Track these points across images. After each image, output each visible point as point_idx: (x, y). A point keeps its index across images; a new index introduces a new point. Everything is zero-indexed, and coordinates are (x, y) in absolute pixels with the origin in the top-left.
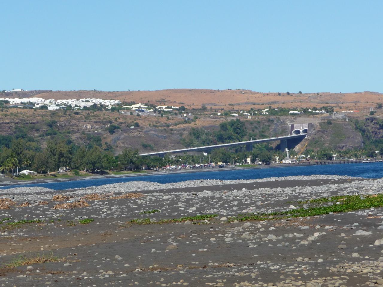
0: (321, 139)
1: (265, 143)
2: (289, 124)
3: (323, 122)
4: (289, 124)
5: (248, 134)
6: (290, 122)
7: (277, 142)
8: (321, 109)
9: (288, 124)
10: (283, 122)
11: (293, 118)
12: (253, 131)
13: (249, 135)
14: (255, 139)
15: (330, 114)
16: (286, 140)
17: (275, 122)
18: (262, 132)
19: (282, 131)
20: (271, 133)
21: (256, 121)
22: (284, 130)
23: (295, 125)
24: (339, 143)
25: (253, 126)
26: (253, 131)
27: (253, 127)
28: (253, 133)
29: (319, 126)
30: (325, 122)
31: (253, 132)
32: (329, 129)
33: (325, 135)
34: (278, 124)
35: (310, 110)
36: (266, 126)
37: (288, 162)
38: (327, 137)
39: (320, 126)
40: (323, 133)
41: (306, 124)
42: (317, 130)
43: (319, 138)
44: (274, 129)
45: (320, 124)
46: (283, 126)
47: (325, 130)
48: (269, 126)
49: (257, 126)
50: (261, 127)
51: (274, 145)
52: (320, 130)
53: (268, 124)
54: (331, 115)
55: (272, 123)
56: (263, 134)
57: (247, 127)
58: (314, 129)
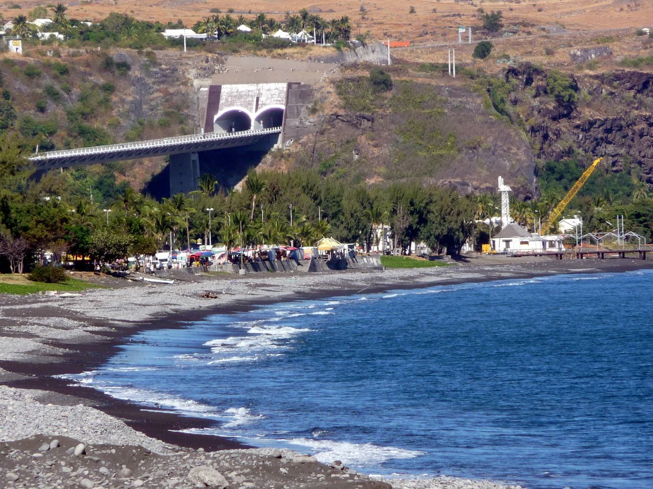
0: (346, 156)
1: (97, 169)
2: (202, 86)
3: (352, 80)
4: (202, 86)
5: (17, 124)
6: (198, 76)
7: (146, 161)
8: (292, 25)
9: (196, 83)
10: (171, 76)
11: (210, 55)
12: (42, 110)
13: (22, 129)
14: (51, 148)
15: (338, 48)
16: (195, 157)
17: (135, 72)
18: (79, 117)
19: (167, 114)
20: (121, 120)
21: (48, 66)
22: (179, 108)
23: (226, 89)
24: (430, 173)
25: (38, 86)
26: (42, 110)
27: (40, 91)
28: (39, 118)
29: (334, 98)
30: (360, 79)
31: (40, 114)
32: (380, 111)
33: (363, 137)
34: (150, 81)
35: (243, 28)
36: (93, 88)
37: (525, 249)
38: (376, 146)
39: (339, 94)
40: (355, 126)
41: (272, 86)
42: (328, 111)
43: (339, 150)
44: (132, 102)
45: (338, 87)
46: (171, 90)
47: (366, 114)
48: (109, 89)
49: (57, 87)
50: (76, 91)
51: (135, 177)
52: (341, 112)
53: (102, 81)
55: (124, 75)
56: (85, 124)
57: (13, 92)
58: (314, 111)
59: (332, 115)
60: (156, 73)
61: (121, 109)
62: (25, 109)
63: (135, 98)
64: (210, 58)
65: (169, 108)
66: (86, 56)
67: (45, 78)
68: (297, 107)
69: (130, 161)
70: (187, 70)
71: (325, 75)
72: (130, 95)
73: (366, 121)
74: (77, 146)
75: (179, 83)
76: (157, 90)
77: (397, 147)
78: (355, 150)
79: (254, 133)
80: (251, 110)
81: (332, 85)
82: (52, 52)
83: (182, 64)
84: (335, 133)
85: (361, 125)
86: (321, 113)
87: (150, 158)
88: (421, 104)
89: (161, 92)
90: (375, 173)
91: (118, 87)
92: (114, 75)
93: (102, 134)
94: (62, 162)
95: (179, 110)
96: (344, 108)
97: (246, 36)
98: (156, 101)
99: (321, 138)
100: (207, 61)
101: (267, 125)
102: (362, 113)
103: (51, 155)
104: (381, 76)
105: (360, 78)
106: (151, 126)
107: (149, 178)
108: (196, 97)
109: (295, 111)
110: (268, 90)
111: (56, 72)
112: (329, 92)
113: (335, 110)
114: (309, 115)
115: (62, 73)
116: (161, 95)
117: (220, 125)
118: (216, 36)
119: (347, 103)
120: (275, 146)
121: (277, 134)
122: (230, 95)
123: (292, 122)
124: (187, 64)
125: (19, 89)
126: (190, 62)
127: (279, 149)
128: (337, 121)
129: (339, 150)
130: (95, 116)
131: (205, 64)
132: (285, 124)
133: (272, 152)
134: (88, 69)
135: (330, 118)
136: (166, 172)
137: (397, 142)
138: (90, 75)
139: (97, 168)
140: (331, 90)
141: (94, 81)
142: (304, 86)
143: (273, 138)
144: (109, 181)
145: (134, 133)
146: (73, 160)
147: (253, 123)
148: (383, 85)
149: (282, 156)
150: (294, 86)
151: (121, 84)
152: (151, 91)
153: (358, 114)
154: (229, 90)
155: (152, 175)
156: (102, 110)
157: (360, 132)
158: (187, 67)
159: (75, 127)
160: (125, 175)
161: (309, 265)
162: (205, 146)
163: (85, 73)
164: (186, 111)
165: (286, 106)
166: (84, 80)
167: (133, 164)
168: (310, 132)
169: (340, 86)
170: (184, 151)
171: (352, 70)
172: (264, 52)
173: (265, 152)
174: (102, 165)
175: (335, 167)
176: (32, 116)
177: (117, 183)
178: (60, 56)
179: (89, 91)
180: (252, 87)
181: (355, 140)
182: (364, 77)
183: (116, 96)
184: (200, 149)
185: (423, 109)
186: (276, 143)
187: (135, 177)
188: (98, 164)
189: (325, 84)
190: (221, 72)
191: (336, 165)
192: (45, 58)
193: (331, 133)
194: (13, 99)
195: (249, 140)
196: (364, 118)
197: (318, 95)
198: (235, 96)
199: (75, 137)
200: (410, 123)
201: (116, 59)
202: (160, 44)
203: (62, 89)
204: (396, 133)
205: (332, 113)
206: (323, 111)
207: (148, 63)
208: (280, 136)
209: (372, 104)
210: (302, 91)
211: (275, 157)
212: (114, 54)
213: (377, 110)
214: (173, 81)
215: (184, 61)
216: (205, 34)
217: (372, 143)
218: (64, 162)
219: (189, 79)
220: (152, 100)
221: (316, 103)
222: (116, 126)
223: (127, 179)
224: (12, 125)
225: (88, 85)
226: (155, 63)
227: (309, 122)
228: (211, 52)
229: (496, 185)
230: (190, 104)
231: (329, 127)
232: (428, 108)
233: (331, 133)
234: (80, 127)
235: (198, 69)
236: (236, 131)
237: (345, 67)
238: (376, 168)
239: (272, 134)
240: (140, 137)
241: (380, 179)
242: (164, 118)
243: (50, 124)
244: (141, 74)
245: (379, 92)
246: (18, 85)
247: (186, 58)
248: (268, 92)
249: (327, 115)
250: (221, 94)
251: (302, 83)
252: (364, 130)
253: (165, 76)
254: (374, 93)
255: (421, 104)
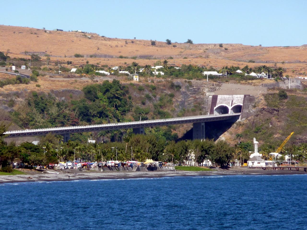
0: (267, 125)
1: (165, 128)
2: (209, 95)
3: (271, 94)
4: (209, 95)
5: (133, 109)
6: (209, 91)
7: (185, 125)
8: (259, 70)
9: (207, 94)
10: (197, 91)
11: (215, 83)
12: (144, 104)
13: (135, 111)
14: (146, 119)
15: (276, 80)
16: (203, 124)
17: (183, 90)
18: (159, 107)
19: (195, 106)
20: (176, 109)
21: (148, 86)
22: (200, 104)
23: (219, 97)
24: (300, 133)
25: (143, 94)
26: (144, 104)
27: (143, 96)
28: (143, 107)
29: (263, 101)
30: (274, 94)
31: (143, 106)
32: (282, 107)
33: (274, 118)
34: (189, 93)
35: (239, 71)
36: (166, 95)
37: (259, 165)
38: (279, 122)
39: (265, 100)
40: (271, 113)
41: (239, 96)
42: (260, 107)
43: (264, 123)
44: (181, 101)
45: (265, 97)
46: (197, 97)
47: (276, 108)
48: (172, 96)
49: (151, 95)
50: (158, 97)
51: (180, 131)
52: (266, 107)
53: (169, 93)
54: (278, 82)
55: (178, 90)
56: (161, 110)
57: (132, 96)
58: (255, 107)
59: (262, 108)
60: (192, 90)
61: (176, 104)
62: (137, 103)
63: (182, 100)
64: (214, 84)
65: (196, 104)
66: (164, 82)
67: (146, 91)
68: (248, 105)
69: (179, 125)
70: (204, 89)
71: (260, 92)
72: (180, 98)
73: (275, 111)
74: (157, 119)
75: (200, 94)
76: (191, 97)
77: (288, 122)
78: (270, 123)
79: (230, 115)
80: (229, 106)
81: (263, 96)
82: (150, 81)
83: (202, 87)
84: (263, 116)
85: (273, 113)
86: (257, 108)
87: (187, 124)
88: (299, 105)
89: (193, 97)
90: (278, 133)
91: (176, 95)
92: (174, 90)
93: (168, 114)
94: (151, 124)
95: (200, 105)
96: (267, 106)
97: (238, 75)
98: (191, 101)
99: (256, 118)
100: (213, 85)
101: (235, 112)
102: (274, 108)
103: (145, 122)
104: (282, 93)
105: (275, 94)
106: (188, 111)
107: (185, 132)
108: (207, 100)
109: (247, 106)
110: (237, 98)
111: (150, 89)
112: (261, 99)
113: (263, 106)
114: (253, 108)
115: (153, 89)
116: (193, 99)
117: (216, 111)
118: (226, 74)
119: (268, 104)
120: (238, 120)
121: (239, 116)
122: (221, 99)
123: (245, 111)
124: (204, 86)
125: (135, 95)
126: (206, 86)
127: (239, 122)
128: (264, 111)
129: (264, 123)
130: (165, 107)
131: (212, 87)
132: (242, 112)
133: (236, 123)
134: (164, 88)
135: (261, 110)
136: (191, 131)
137: (288, 120)
138: (165, 90)
139: (165, 128)
140: (262, 98)
141: (166, 92)
142: (251, 96)
143: (237, 117)
144: (169, 133)
145: (181, 114)
146: (155, 124)
147: (230, 111)
148: (284, 97)
149: (240, 125)
150: (247, 96)
151: (177, 94)
152: (189, 97)
153: (272, 108)
154: (221, 97)
155: (187, 131)
156: (169, 104)
157: (273, 116)
158: (204, 88)
159: (157, 111)
160: (176, 131)
161: (136, 168)
162: (208, 120)
163: (163, 89)
164: (202, 105)
165: (243, 104)
166: (162, 92)
167: (180, 126)
168: (252, 115)
169: (266, 97)
170: (198, 121)
171: (272, 90)
172: (244, 82)
173: (233, 123)
174: (167, 126)
175: (262, 130)
176: (140, 106)
177: (172, 134)
178: (154, 82)
179: (164, 97)
180: (231, 96)
181: (270, 119)
182: (276, 93)
183: (175, 99)
184: (205, 121)
185: (300, 107)
186: (238, 119)
187: (180, 131)
188: (165, 126)
189: (260, 96)
190: (219, 90)
191: (262, 129)
192: (147, 83)
193: (261, 116)
194: (132, 99)
195: (224, 118)
196: (275, 110)
197: (257, 100)
198: (223, 100)
199: (157, 115)
200: (294, 113)
201: (175, 84)
202: (200, 78)
203: (152, 96)
204: (287, 116)
205: (261, 108)
206: (258, 107)
207: (188, 86)
208: (240, 116)
209: (278, 105)
210: (250, 98)
211: (237, 125)
212: (175, 82)
213: (280, 107)
214: (198, 93)
215: (203, 85)
216: (221, 74)
217: (277, 120)
218: (152, 125)
219: (205, 92)
220: (189, 101)
221: (256, 103)
222: (173, 111)
223: (176, 132)
224: (131, 110)
225: (164, 94)
226: (191, 86)
227: (253, 111)
228: (215, 82)
229: (253, 142)
230: (204, 103)
231: (260, 113)
232: (302, 107)
233: (261, 116)
234: (159, 111)
235: (209, 88)
236: (222, 114)
237: (269, 89)
238: (278, 130)
239: (237, 115)
240: (183, 116)
241: (280, 135)
242: (193, 108)
243: (146, 109)
244: (185, 90)
245: (282, 99)
246: (135, 93)
247: (204, 84)
248: (237, 98)
249: (260, 108)
250: (218, 99)
251: (251, 95)
252: (275, 115)
253: (195, 91)
254: (280, 100)
255: (299, 105)
